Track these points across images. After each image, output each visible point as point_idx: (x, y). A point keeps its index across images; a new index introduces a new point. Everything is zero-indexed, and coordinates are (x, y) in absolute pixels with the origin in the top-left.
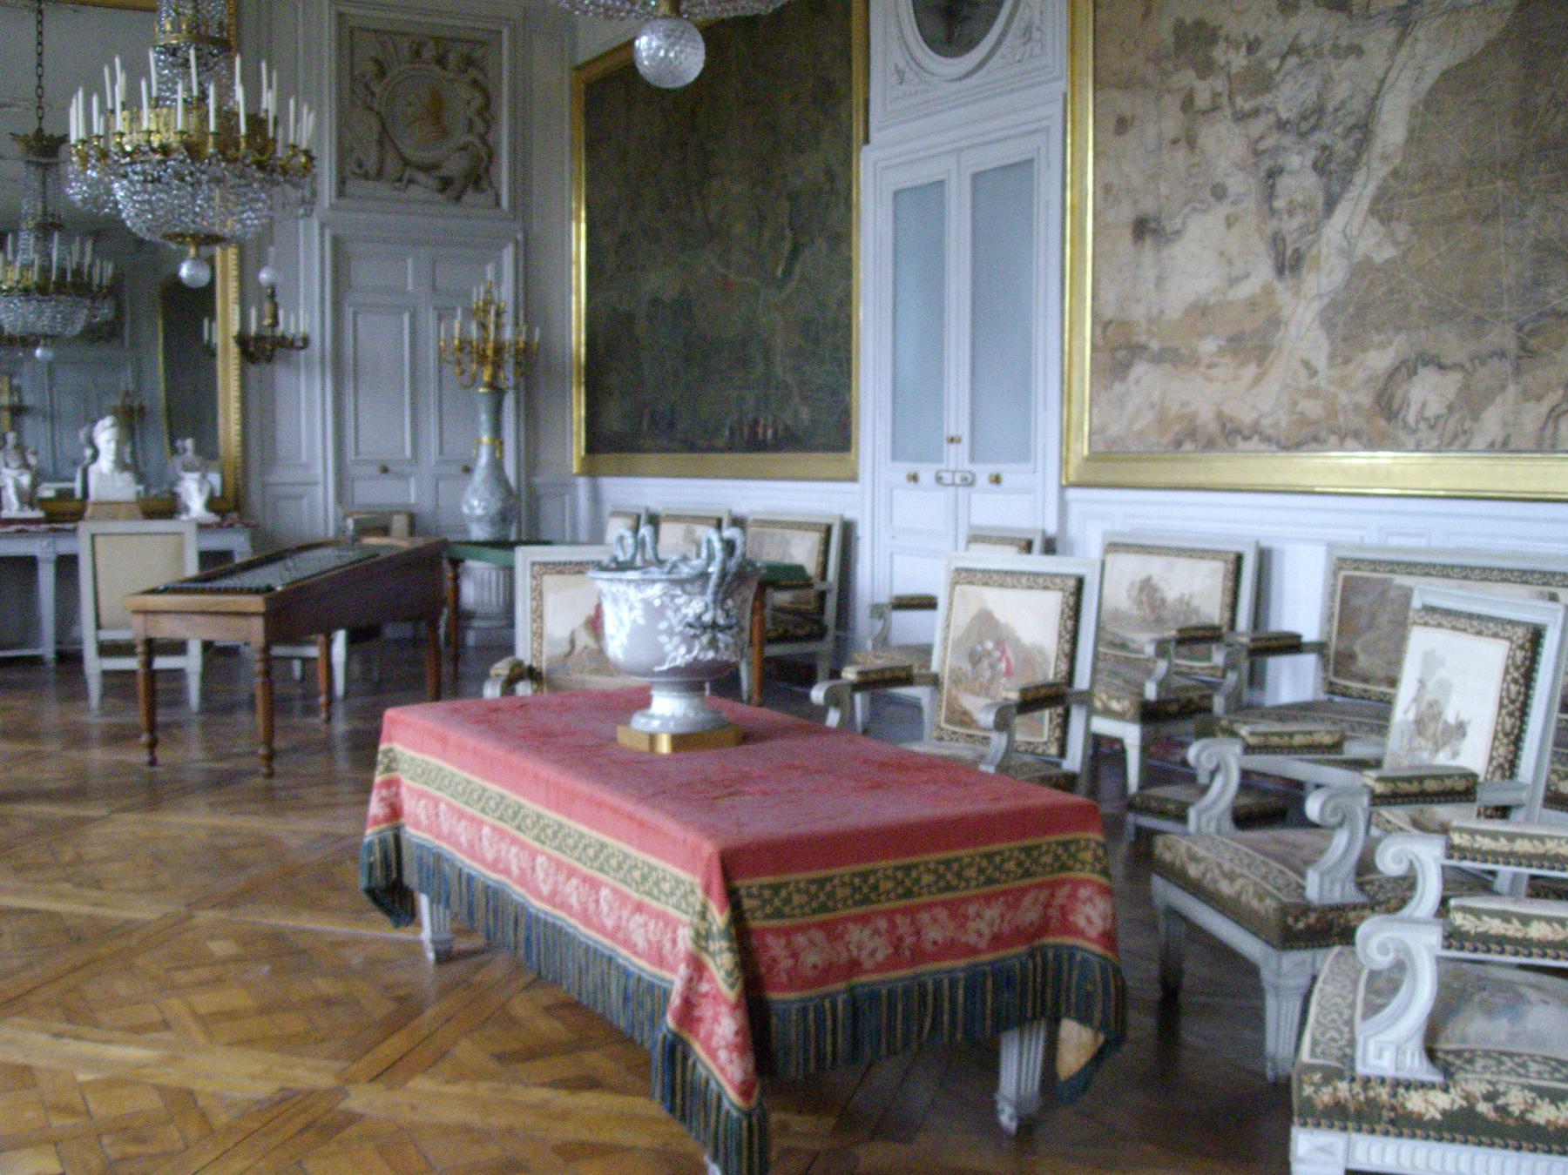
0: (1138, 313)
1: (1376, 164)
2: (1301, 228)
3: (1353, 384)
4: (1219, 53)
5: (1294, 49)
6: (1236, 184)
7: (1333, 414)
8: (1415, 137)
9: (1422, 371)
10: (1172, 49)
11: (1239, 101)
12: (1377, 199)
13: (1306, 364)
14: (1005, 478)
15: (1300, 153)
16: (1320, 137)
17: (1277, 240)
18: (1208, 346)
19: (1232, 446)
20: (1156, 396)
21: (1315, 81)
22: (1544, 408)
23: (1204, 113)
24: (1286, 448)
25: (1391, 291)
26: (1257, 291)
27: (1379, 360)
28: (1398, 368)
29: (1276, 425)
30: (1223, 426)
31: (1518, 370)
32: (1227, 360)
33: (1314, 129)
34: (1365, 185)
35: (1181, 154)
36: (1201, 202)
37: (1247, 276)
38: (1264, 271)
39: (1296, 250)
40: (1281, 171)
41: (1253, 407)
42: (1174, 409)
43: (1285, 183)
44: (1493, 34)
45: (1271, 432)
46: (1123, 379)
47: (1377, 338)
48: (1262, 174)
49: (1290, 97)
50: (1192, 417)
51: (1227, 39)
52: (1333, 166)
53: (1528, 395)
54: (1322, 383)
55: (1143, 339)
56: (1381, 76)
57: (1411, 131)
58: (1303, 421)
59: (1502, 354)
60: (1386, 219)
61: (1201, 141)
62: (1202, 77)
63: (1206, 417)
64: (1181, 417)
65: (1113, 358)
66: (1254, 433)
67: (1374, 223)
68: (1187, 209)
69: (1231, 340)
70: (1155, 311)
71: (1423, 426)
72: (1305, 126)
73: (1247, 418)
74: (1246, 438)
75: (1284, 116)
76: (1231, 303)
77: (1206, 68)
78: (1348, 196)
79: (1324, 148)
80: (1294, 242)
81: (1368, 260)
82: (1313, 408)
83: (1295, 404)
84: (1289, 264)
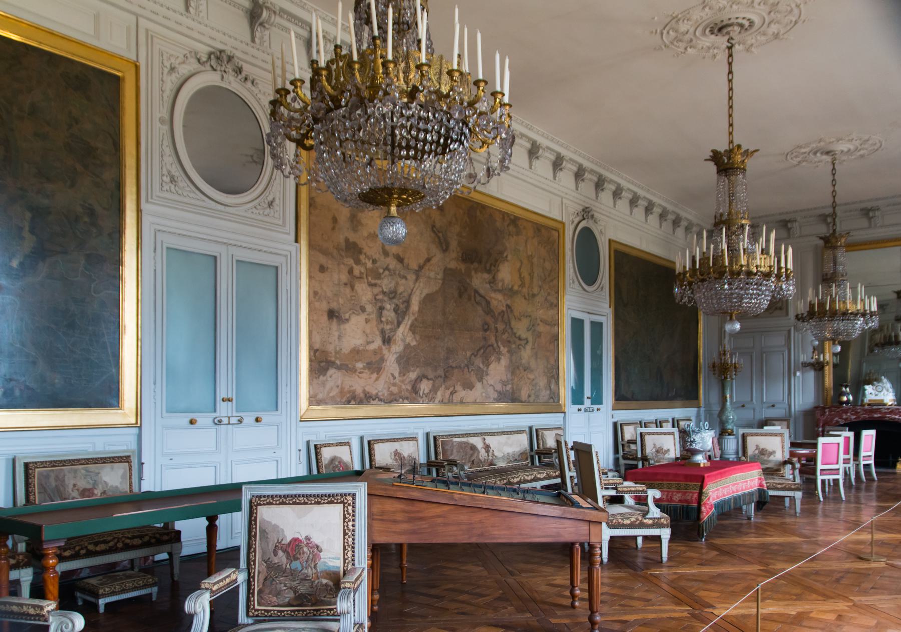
0: (331, 348)
1: (411, 315)
2: (390, 329)
3: (406, 382)
6: (369, 308)
7: (401, 392)
8: (420, 311)
9: (423, 380)
10: (344, 247)
11: (370, 279)
12: (412, 326)
13: (393, 375)
14: (265, 420)
15: (390, 304)
16: (395, 301)
17: (383, 332)
18: (360, 365)
19: (369, 402)
20: (340, 382)
23: (357, 278)
24: (386, 403)
25: (416, 355)
26: (377, 348)
27: (413, 376)
28: (418, 379)
29: (383, 395)
30: (366, 395)
32: (367, 371)
33: (394, 298)
34: (408, 320)
35: (348, 290)
36: (356, 311)
37: (373, 342)
38: (378, 342)
39: (389, 336)
40: (384, 308)
41: (376, 389)
42: (347, 388)
43: (385, 312)
44: (438, 288)
45: (382, 397)
46: (325, 375)
47: (412, 369)
48: (378, 307)
49: (387, 283)
50: (354, 392)
51: (365, 254)
52: (399, 312)
54: (398, 382)
55: (333, 359)
56: (412, 288)
57: (420, 308)
58: (392, 394)
59: (441, 377)
60: (414, 333)
61: (356, 287)
63: (359, 391)
64: (349, 392)
65: (319, 365)
66: (376, 397)
67: (411, 333)
68: (351, 312)
69: (368, 364)
70: (338, 349)
71: (424, 396)
72: (392, 296)
73: (374, 392)
74: (374, 400)
75: (385, 290)
76: (368, 351)
77: (358, 262)
78: (404, 323)
79: (397, 305)
80: (390, 333)
81: (409, 344)
82: (395, 390)
83: (389, 388)
84: (387, 341)
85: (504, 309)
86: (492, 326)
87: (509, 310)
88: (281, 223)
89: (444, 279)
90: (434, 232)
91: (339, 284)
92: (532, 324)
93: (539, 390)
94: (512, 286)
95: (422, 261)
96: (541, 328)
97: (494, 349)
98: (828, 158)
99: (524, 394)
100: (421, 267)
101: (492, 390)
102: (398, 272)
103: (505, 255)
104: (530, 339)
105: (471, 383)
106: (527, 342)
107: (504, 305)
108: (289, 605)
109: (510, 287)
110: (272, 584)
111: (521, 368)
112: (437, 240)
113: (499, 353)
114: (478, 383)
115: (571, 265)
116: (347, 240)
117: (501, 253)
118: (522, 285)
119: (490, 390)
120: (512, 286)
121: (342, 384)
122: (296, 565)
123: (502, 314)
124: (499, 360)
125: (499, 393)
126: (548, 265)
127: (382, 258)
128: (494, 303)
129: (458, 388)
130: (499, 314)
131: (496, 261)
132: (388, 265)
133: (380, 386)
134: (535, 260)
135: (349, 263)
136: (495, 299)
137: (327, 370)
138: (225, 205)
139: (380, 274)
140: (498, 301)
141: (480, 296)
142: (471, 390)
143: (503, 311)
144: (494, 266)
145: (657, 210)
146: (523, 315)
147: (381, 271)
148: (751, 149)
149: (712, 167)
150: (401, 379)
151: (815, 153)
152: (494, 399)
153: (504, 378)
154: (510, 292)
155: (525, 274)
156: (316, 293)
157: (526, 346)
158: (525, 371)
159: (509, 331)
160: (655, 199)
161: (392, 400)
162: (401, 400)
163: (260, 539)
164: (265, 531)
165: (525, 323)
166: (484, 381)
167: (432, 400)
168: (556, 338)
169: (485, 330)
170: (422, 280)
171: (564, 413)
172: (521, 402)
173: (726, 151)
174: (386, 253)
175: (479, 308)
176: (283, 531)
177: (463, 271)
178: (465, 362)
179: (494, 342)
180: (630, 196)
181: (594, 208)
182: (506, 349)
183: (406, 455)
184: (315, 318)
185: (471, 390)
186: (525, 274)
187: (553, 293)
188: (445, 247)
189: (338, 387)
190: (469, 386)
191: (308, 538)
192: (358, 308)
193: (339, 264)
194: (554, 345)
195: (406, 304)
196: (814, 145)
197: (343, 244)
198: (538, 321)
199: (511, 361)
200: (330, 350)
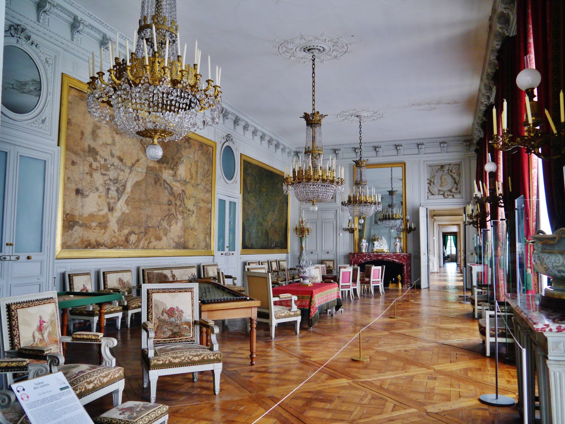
0: (76, 213)
1: (126, 194)
5: (113, 165)
6: (101, 189)
7: (118, 241)
8: (132, 191)
10: (87, 151)
11: (102, 170)
12: (126, 201)
13: (114, 231)
16: (117, 185)
17: (109, 204)
18: (94, 224)
19: (98, 248)
20: (81, 235)
21: (117, 173)
22: (147, 242)
23: (95, 170)
25: (128, 219)
27: (126, 231)
31: (145, 235)
32: (98, 228)
33: (116, 183)
38: (106, 210)
40: (110, 189)
42: (85, 239)
43: (110, 192)
44: (142, 178)
45: (107, 245)
46: (72, 230)
47: (126, 227)
49: (112, 174)
50: (90, 241)
52: (119, 192)
55: (78, 220)
57: (131, 190)
58: (113, 243)
60: (127, 205)
61: (93, 176)
62: (95, 161)
63: (93, 241)
64: (87, 241)
68: (90, 191)
70: (81, 214)
72: (115, 182)
73: (102, 241)
74: (102, 246)
75: (111, 178)
77: (95, 160)
79: (118, 188)
82: (115, 240)
84: (111, 209)
85: (181, 192)
86: (174, 203)
87: (183, 193)
88: (49, 133)
89: (146, 173)
90: (142, 144)
91: (83, 173)
94: (186, 179)
95: (134, 162)
96: (202, 204)
97: (174, 216)
98: (358, 119)
99: (190, 244)
100: (133, 165)
101: (172, 242)
102: (119, 167)
103: (182, 160)
104: (195, 211)
108: (169, 337)
109: (184, 179)
110: (161, 329)
111: (189, 228)
112: (143, 149)
113: (177, 219)
115: (219, 168)
116: (89, 146)
117: (180, 158)
118: (192, 178)
119: (171, 241)
120: (186, 179)
121: (83, 236)
122: (172, 319)
124: (177, 223)
125: (177, 243)
126: (206, 167)
127: (110, 158)
128: (175, 189)
129: (153, 239)
130: (178, 195)
131: (177, 163)
132: (114, 163)
133: (105, 238)
134: (199, 164)
135: (90, 160)
136: (176, 186)
137: (73, 226)
138: (15, 120)
139: (108, 168)
140: (177, 187)
142: (160, 241)
143: (180, 194)
145: (267, 138)
147: (109, 166)
148: (324, 115)
149: (304, 122)
150: (119, 233)
151: (352, 116)
152: (174, 247)
153: (180, 234)
154: (185, 183)
155: (193, 172)
156: (68, 178)
159: (183, 205)
160: (266, 132)
162: (118, 247)
163: (154, 308)
164: (157, 305)
165: (193, 201)
167: (137, 247)
168: (210, 211)
169: (170, 205)
170: (133, 173)
171: (214, 256)
172: (189, 249)
173: (311, 114)
174: (112, 155)
175: (166, 191)
176: (166, 304)
177: (158, 168)
178: (157, 224)
179: (174, 212)
180: (253, 130)
181: (232, 135)
182: (181, 217)
183: (125, 281)
184: (68, 193)
185: (160, 241)
186: (193, 172)
187: (209, 184)
189: (80, 237)
190: (159, 239)
191: (177, 308)
193: (83, 161)
195: (123, 187)
196: (351, 112)
197: (87, 148)
199: (184, 224)
200: (76, 214)
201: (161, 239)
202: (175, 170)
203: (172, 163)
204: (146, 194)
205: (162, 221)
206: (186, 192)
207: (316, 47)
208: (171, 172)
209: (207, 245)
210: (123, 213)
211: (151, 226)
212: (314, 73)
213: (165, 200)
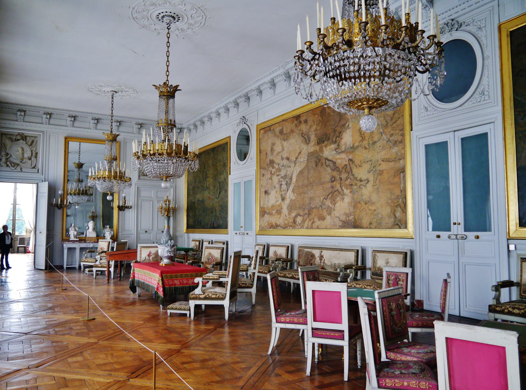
0: (265, 206)
4: (275, 165)
5: (283, 166)
7: (289, 223)
12: (293, 190)
16: (286, 179)
17: (282, 195)
24: (283, 228)
27: (293, 215)
33: (286, 178)
35: (270, 180)
38: (280, 200)
43: (282, 186)
44: (304, 166)
49: (283, 173)
50: (272, 223)
53: (310, 220)
58: (285, 224)
60: (294, 193)
61: (273, 179)
62: (273, 169)
63: (274, 224)
73: (279, 224)
81: (292, 199)
82: (286, 222)
84: (283, 199)
85: (347, 163)
87: (351, 163)
92: (372, 166)
93: (381, 218)
94: (353, 145)
95: (297, 155)
97: (339, 193)
99: (365, 221)
100: (297, 158)
105: (324, 216)
106: (368, 181)
107: (347, 160)
109: (351, 146)
111: (362, 202)
113: (344, 194)
114: (328, 216)
117: (344, 125)
119: (337, 220)
123: (346, 166)
124: (343, 199)
125: (343, 222)
127: (281, 162)
128: (339, 162)
129: (316, 220)
130: (343, 168)
133: (280, 221)
140: (342, 159)
141: (329, 160)
142: (323, 221)
143: (346, 165)
144: (339, 137)
146: (364, 162)
152: (340, 226)
157: (367, 185)
158: (366, 204)
159: (352, 177)
161: (285, 227)
166: (332, 214)
167: (302, 227)
169: (333, 182)
177: (318, 150)
178: (320, 204)
185: (323, 221)
188: (308, 142)
190: (322, 218)
192: (273, 187)
194: (400, 178)
198: (380, 162)
199: (353, 198)
201: (325, 219)
202: (338, 142)
203: (334, 135)
204: (308, 179)
205: (324, 200)
206: (354, 160)
207: (167, 14)
208: (333, 146)
209: (397, 222)
210: (291, 200)
211: (313, 207)
212: (112, 104)
213: (327, 178)
